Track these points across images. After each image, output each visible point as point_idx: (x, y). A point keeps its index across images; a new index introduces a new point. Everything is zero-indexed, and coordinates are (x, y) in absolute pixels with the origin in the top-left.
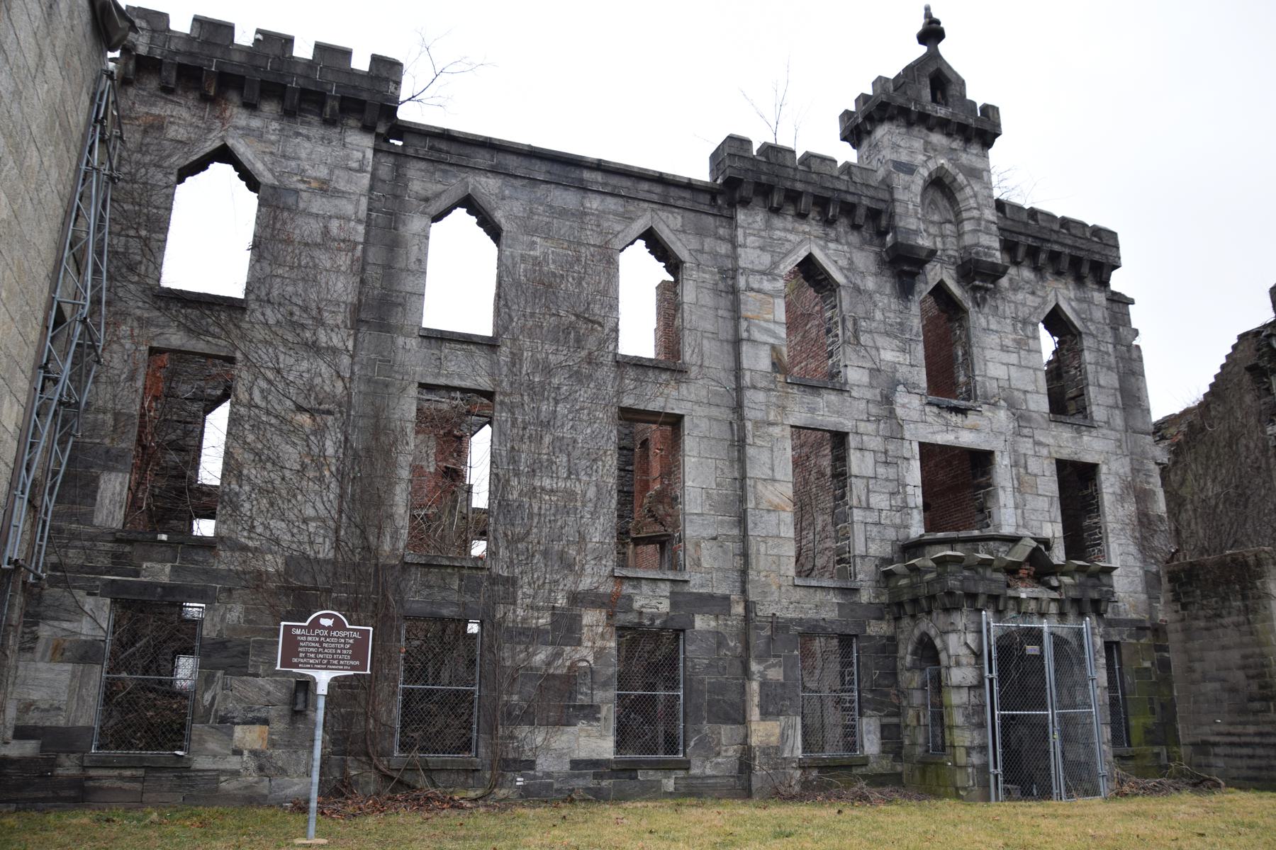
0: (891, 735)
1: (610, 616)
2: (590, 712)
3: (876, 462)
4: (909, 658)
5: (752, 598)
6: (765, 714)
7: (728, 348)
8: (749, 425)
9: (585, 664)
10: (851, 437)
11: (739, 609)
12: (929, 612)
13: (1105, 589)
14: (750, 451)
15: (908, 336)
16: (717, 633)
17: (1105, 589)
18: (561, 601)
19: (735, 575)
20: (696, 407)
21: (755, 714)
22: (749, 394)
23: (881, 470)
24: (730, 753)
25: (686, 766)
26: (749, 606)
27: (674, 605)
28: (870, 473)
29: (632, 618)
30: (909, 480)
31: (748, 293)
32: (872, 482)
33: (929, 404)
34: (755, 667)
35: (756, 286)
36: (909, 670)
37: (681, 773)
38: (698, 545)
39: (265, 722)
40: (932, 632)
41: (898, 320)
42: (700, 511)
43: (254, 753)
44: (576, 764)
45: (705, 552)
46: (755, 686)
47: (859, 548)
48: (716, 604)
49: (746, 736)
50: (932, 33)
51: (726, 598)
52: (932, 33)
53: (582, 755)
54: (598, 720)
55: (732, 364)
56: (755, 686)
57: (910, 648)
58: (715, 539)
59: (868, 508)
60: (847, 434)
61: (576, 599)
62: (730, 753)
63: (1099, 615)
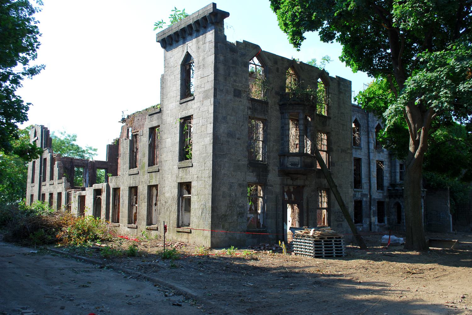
0: (388, 220)
4: (392, 206)
5: (372, 194)
6: (373, 216)
7: (367, 144)
8: (371, 161)
10: (384, 162)
11: (369, 196)
12: (399, 198)
14: (371, 165)
16: (366, 201)
19: (368, 190)
21: (372, 217)
22: (371, 154)
24: (368, 223)
25: (363, 226)
26: (371, 196)
28: (386, 170)
34: (372, 208)
36: (392, 208)
37: (362, 227)
38: (364, 184)
40: (400, 202)
42: (364, 177)
45: (365, 186)
46: (372, 211)
47: (385, 185)
48: (365, 195)
49: (370, 220)
51: (367, 194)
55: (367, 147)
56: (372, 211)
57: (393, 204)
58: (366, 183)
59: (386, 177)
60: (383, 161)
62: (368, 223)
63: (423, 198)
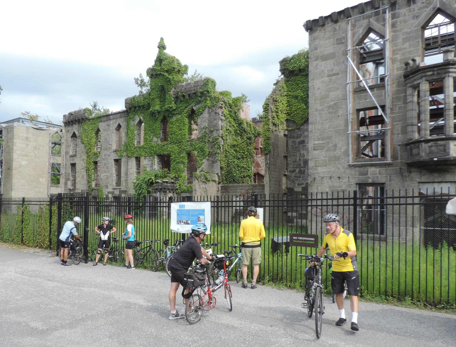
1: (112, 195)
18: (107, 193)
27: (119, 193)
29: (114, 195)
52: (162, 47)
61: (109, 193)
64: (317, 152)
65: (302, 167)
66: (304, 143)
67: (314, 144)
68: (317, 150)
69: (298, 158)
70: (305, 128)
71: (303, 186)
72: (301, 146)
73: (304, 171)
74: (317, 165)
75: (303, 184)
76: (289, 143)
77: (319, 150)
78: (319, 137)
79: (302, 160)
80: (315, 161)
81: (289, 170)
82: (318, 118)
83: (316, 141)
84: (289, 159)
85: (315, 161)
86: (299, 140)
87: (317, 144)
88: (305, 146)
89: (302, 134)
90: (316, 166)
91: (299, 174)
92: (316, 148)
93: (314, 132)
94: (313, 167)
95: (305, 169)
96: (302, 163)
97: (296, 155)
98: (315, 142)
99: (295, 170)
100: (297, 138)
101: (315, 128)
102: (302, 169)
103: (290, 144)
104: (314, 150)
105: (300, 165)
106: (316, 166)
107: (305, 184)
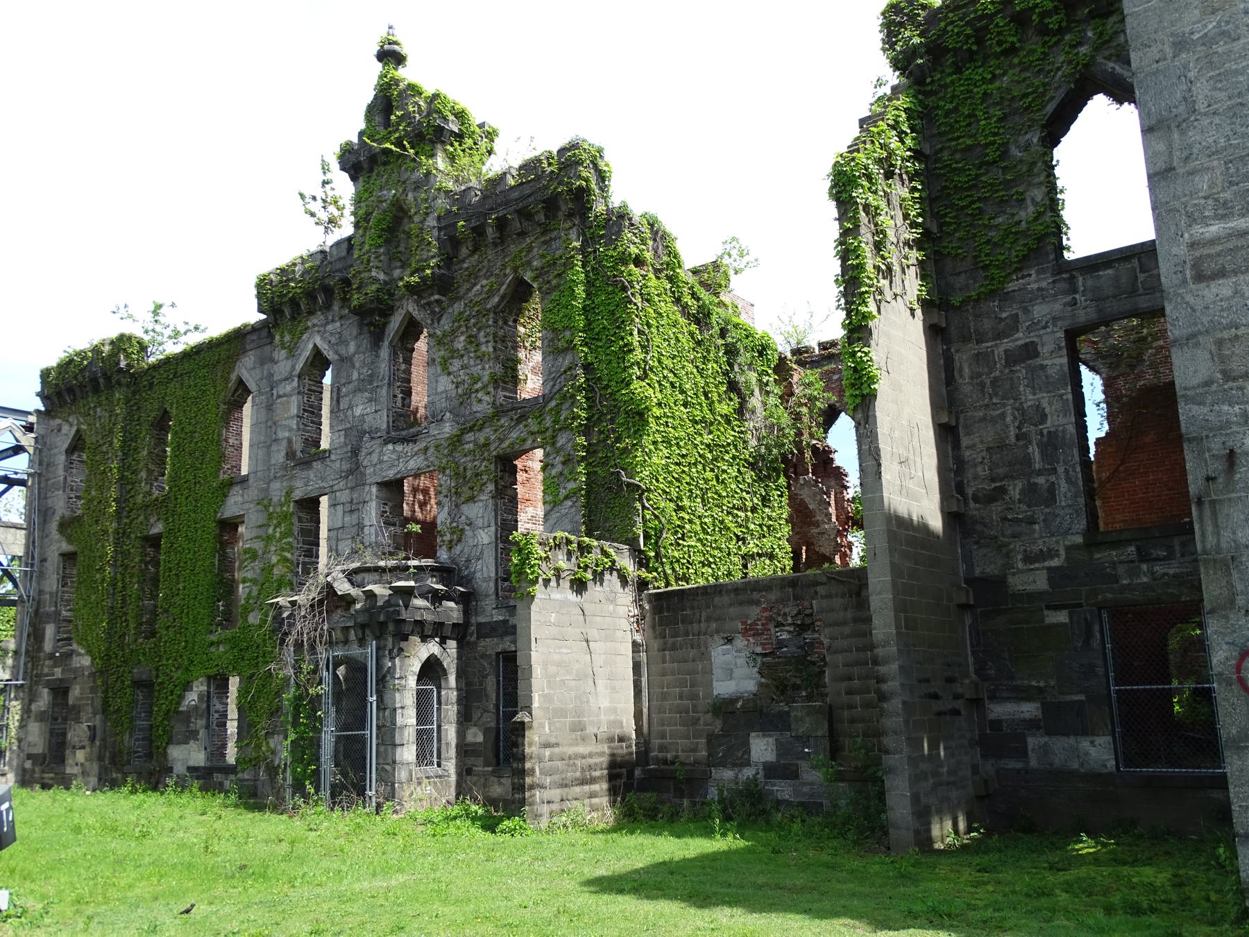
2: (193, 735)
3: (344, 512)
9: (193, 703)
13: (392, 609)
15: (375, 385)
17: (392, 609)
20: (252, 506)
23: (347, 519)
30: (367, 523)
31: (279, 401)
32: (341, 531)
33: (386, 442)
35: (281, 393)
39: (83, 747)
41: (370, 372)
43: (82, 764)
44: (190, 769)
50: (390, 56)
52: (390, 56)
53: (192, 763)
54: (198, 740)
64: (1222, 288)
65: (1039, 473)
66: (1037, 355)
67: (1192, 245)
68: (1221, 273)
69: (1012, 432)
70: (1035, 286)
71: (1055, 563)
72: (1021, 371)
73: (1052, 489)
74: (1236, 366)
75: (1052, 554)
76: (957, 364)
77: (1235, 273)
78: (1227, 195)
79: (1035, 438)
80: (1220, 343)
81: (970, 491)
82: (1202, 91)
83: (1205, 222)
84: (965, 441)
85: (1220, 343)
86: (1006, 344)
87: (1213, 242)
88: (1043, 367)
89: (1022, 317)
90: (1228, 376)
91: (1024, 507)
92: (1209, 267)
93: (1181, 171)
94: (1208, 383)
95: (1052, 478)
96: (1034, 451)
97: (1003, 415)
98: (1198, 230)
99: (1002, 491)
100: (999, 336)
101: (1190, 146)
102: (1041, 480)
103: (966, 371)
104: (1200, 277)
105: (1028, 460)
106: (1228, 376)
107: (1062, 553)
